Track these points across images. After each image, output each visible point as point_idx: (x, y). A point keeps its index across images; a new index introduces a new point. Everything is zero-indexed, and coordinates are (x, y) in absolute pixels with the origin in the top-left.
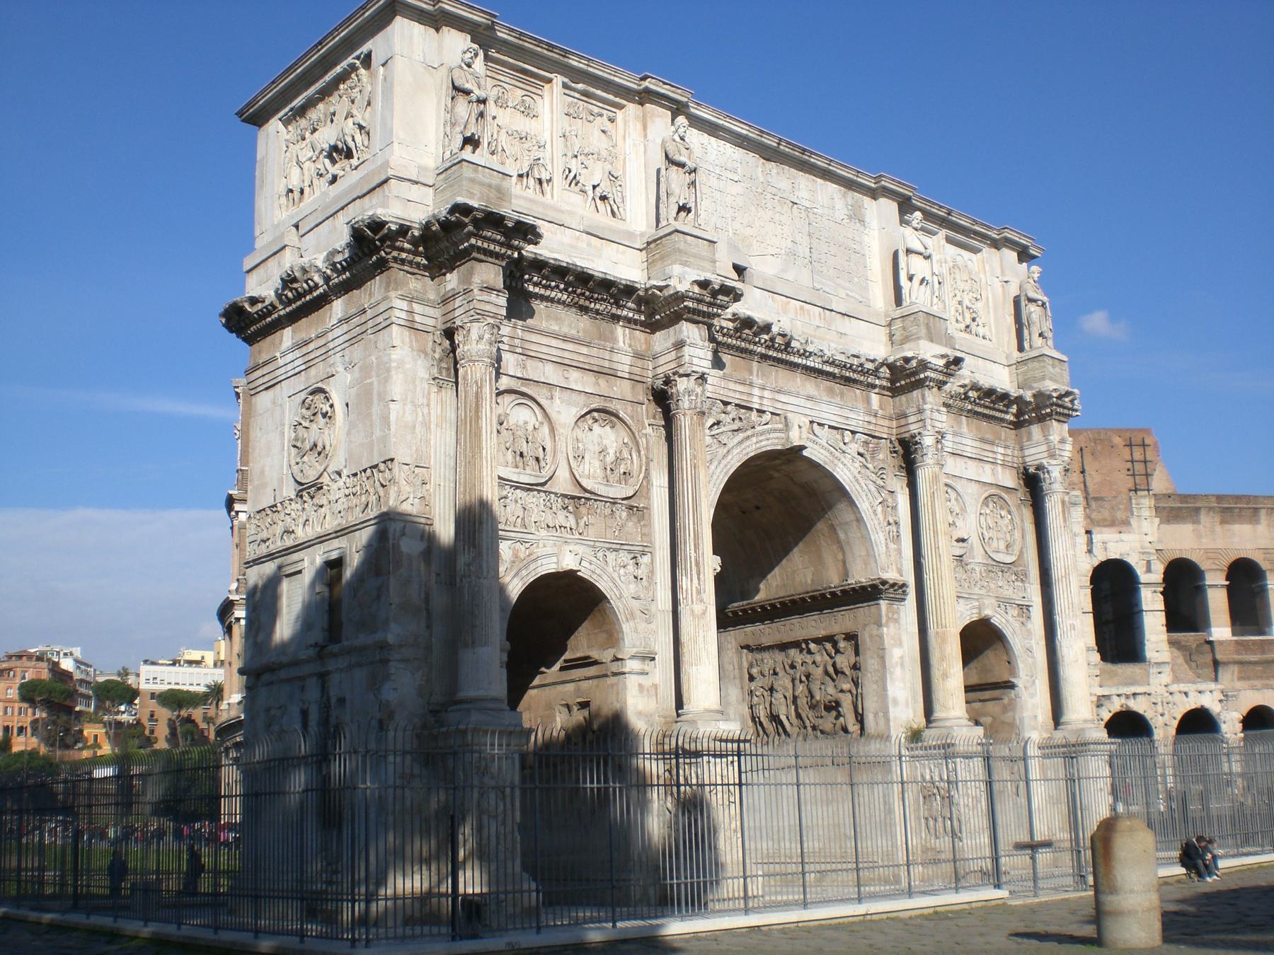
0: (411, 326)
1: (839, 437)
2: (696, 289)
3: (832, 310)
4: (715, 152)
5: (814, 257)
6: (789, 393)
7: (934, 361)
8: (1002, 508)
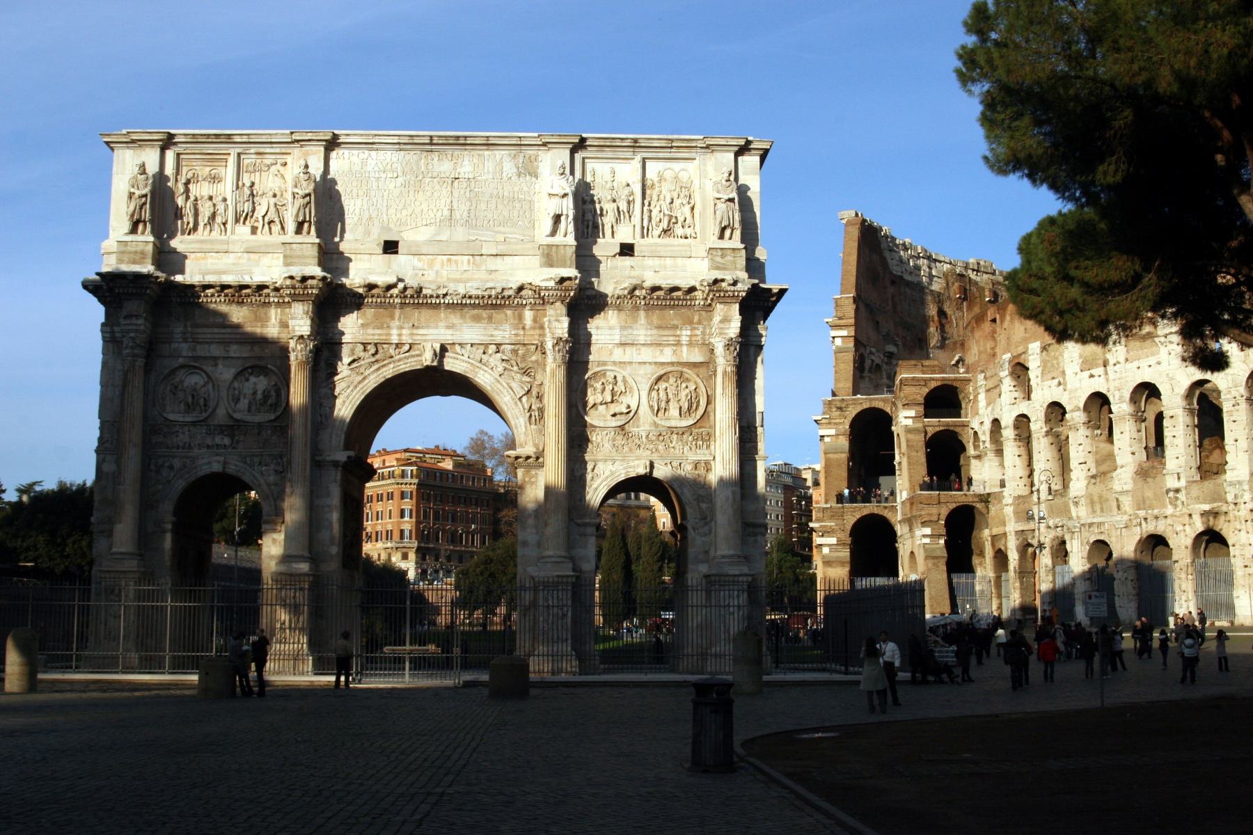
2: (288, 282)
3: (482, 255)
4: (375, 162)
5: (472, 216)
7: (544, 284)
8: (688, 380)
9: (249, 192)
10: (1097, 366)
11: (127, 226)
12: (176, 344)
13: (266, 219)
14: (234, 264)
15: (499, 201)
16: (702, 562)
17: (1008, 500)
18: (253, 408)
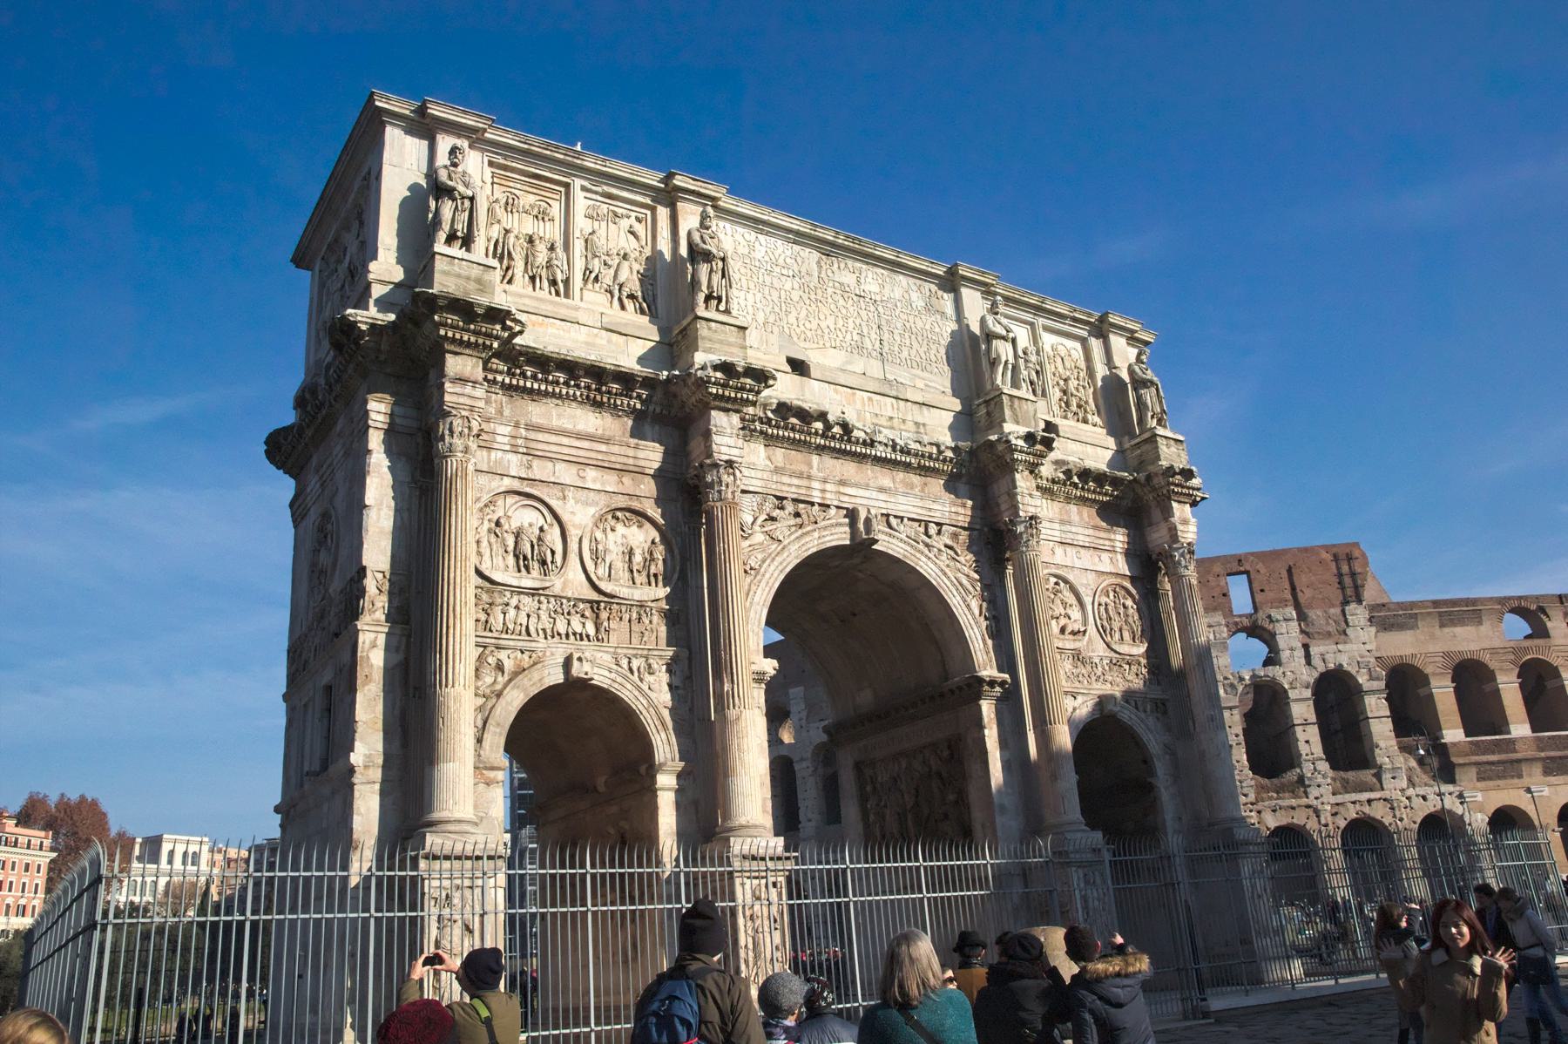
1: (922, 529)
3: (907, 400)
4: (764, 249)
5: (886, 349)
6: (856, 485)
12: (500, 454)
13: (625, 294)
15: (913, 337)
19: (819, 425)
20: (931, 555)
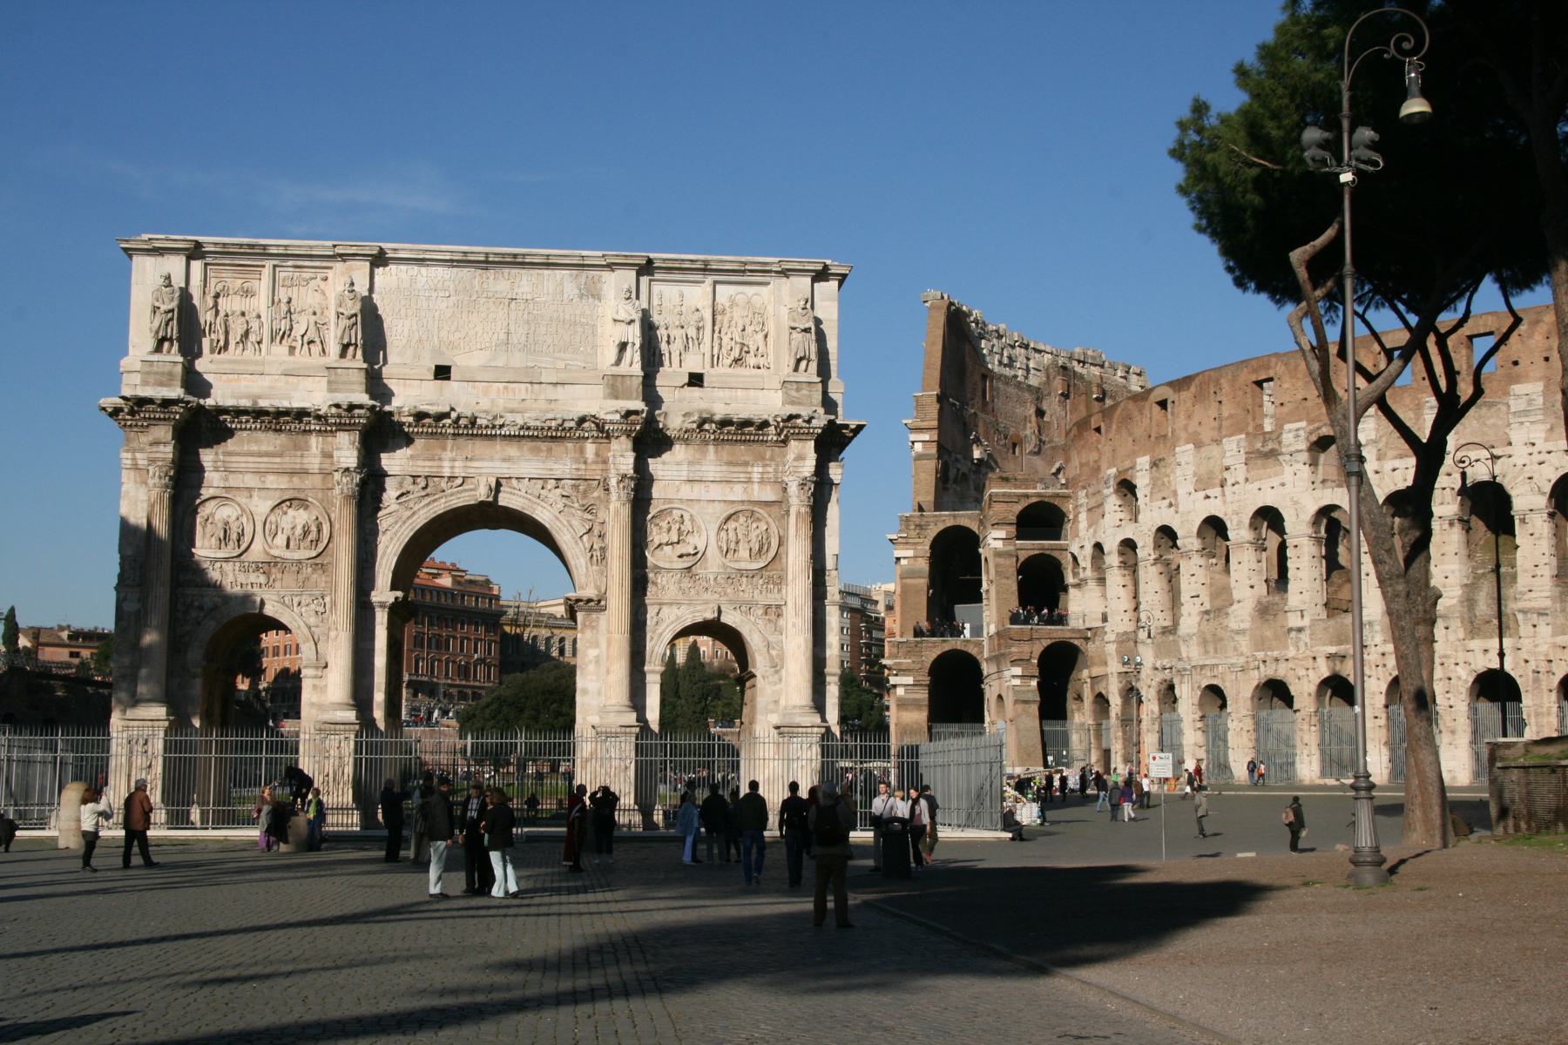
0: (135, 467)
2: (334, 410)
5: (531, 340)
6: (482, 460)
7: (609, 417)
8: (759, 520)
9: (286, 309)
10: (1213, 486)
11: (151, 344)
14: (270, 387)
16: (772, 712)
17: (1111, 637)
18: (292, 544)
19: (448, 421)
20: (545, 505)
